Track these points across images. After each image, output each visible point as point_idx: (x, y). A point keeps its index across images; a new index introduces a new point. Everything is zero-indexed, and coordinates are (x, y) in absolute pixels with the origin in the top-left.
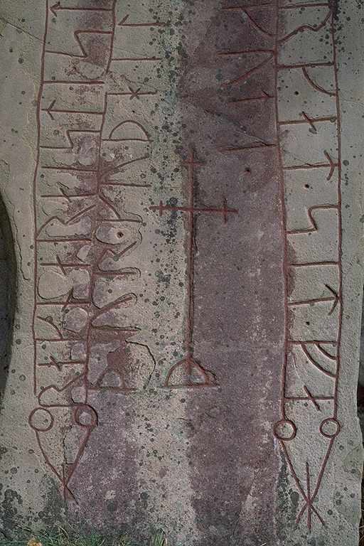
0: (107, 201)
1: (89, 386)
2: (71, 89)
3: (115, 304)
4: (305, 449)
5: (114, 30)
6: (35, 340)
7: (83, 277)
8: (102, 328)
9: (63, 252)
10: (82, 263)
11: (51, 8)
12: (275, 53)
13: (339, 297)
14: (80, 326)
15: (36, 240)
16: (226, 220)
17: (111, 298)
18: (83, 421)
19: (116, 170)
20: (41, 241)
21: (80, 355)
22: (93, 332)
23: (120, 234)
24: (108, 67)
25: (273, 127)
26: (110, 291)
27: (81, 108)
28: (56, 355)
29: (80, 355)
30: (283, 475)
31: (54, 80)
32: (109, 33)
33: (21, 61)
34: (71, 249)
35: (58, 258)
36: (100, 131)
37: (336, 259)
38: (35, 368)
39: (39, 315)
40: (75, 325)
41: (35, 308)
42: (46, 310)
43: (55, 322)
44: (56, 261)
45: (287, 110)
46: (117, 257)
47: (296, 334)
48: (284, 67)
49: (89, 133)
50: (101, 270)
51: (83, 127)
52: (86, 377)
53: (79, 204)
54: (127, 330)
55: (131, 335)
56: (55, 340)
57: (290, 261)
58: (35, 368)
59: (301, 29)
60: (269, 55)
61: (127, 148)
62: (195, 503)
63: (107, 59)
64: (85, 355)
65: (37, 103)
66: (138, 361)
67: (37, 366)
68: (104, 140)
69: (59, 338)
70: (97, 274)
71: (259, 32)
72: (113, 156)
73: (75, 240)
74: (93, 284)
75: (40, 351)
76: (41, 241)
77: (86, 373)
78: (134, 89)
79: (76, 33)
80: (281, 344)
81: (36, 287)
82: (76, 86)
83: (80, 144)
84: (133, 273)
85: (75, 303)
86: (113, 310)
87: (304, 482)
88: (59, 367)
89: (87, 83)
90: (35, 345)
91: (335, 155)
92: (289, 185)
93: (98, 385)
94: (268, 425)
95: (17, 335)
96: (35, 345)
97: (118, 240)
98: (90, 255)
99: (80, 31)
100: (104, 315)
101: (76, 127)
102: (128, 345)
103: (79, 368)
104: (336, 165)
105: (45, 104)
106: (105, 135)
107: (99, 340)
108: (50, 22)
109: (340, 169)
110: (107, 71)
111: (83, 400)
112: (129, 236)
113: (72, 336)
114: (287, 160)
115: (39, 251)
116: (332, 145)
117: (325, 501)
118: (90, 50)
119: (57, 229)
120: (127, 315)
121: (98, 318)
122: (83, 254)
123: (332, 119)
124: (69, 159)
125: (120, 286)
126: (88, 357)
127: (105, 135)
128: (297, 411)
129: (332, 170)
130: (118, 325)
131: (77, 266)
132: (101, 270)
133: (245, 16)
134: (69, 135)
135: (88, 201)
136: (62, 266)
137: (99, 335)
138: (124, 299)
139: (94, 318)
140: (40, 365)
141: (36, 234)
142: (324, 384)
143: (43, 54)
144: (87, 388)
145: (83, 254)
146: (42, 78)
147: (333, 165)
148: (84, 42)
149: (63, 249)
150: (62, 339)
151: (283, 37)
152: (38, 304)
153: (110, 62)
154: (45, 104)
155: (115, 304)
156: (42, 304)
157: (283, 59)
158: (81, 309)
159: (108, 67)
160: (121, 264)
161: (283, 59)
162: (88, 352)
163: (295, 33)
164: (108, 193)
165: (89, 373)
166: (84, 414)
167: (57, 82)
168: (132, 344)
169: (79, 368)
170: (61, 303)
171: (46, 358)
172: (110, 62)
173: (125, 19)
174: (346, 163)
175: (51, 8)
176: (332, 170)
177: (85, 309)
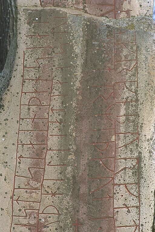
2: (26, 192)
5: (45, 167)
11: (19, 157)
12: (113, 179)
19: (45, 227)
24: (42, 183)
25: (111, 210)
27: (30, 200)
31: (19, 188)
32: (43, 168)
33: (5, 180)
36: (39, 210)
45: (118, 203)
48: (117, 184)
49: (33, 210)
51: (31, 208)
59: (125, 169)
60: (111, 179)
61: (50, 217)
63: (42, 179)
65: (12, 198)
68: (40, 214)
71: (107, 169)
72: (43, 220)
78: (53, 192)
79: (29, 168)
82: (28, 191)
89: (33, 189)
91: (137, 222)
99: (31, 168)
101: (28, 208)
104: (138, 226)
105: (15, 198)
106: (41, 212)
108: (18, 163)
109: (139, 227)
110: (42, 184)
114: (117, 224)
116: (136, 217)
118: (35, 176)
123: (137, 207)
124: (25, 222)
127: (41, 212)
129: (136, 228)
133: (101, 162)
134: (25, 211)
143: (15, 177)
146: (14, 187)
147: (136, 226)
148: (32, 172)
151: (117, 172)
153: (43, 181)
154: (15, 198)
157: (116, 181)
159: (42, 183)
161: (116, 181)
163: (122, 170)
167: (21, 189)
172: (43, 181)
173: (49, 163)
174: (142, 225)
175: (19, 157)
176: (136, 228)
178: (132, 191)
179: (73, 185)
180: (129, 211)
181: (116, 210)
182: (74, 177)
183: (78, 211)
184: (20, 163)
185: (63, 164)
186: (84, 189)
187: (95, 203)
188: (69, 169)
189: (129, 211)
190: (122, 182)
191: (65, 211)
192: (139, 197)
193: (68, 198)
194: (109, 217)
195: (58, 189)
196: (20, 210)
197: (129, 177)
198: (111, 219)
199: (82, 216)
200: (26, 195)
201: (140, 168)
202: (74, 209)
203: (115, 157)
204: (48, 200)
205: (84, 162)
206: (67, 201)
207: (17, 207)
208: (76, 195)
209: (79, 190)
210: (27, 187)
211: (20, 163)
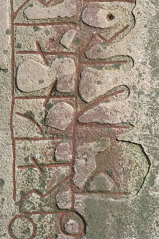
1: (76, 190)
3: (104, 98)
6: (14, 140)
7: (69, 67)
8: (91, 124)
9: (45, 40)
10: (65, 50)
14: (65, 122)
15: (13, 24)
17: (100, 90)
18: (69, 229)
20: (18, 24)
21: (65, 156)
22: (80, 129)
23: (111, 17)
26: (99, 83)
28: (37, 156)
29: (65, 156)
34: (54, 34)
35: (38, 45)
38: (14, 170)
39: (18, 110)
40: (60, 122)
41: (13, 103)
43: (36, 118)
44: (35, 48)
46: (107, 42)
52: (71, 181)
54: (118, 127)
55: (122, 132)
56: (36, 139)
58: (14, 170)
64: (71, 156)
66: (130, 162)
67: (16, 168)
69: (40, 136)
70: (85, 63)
73: (59, 23)
74: (80, 75)
75: (19, 152)
76: (18, 24)
77: (72, 176)
81: (15, 80)
84: (125, 62)
85: (59, 97)
86: (101, 105)
88: (41, 170)
90: (14, 144)
93: (87, 190)
96: (14, 144)
97: (107, 23)
98: (76, 41)
100: (91, 111)
102: (119, 144)
103: (64, 170)
107: (87, 139)
111: (69, 206)
112: (121, 18)
113: (56, 135)
115: (18, 37)
120: (119, 109)
121: (85, 113)
122: (68, 41)
125: (110, 78)
126: (74, 157)
130: (108, 122)
131: (61, 55)
132: (85, 57)
136: (43, 54)
137: (86, 131)
138: (114, 92)
139: (82, 113)
140: (19, 167)
141: (13, 16)
144: (74, 192)
145: (68, 41)
149: (44, 35)
150: (44, 138)
152: (17, 98)
155: (104, 98)
156: (21, 98)
158: (65, 103)
160: (110, 52)
162: (75, 152)
165: (77, 174)
166: (71, 221)
168: (124, 143)
169: (64, 170)
170: (42, 97)
171: (26, 159)
177: (71, 104)
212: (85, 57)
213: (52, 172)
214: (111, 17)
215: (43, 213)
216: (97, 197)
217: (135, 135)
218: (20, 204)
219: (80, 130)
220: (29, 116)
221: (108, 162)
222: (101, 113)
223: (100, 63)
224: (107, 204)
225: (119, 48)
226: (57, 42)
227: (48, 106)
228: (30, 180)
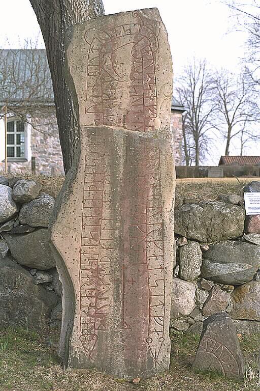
0: (100, 279)
3: (102, 307)
4: (155, 345)
7: (94, 300)
13: (164, 305)
16: (133, 284)
17: (101, 306)
23: (104, 288)
30: (149, 353)
33: (75, 240)
34: (90, 292)
37: (163, 294)
42: (84, 309)
46: (102, 294)
47: (152, 316)
50: (99, 297)
53: (92, 280)
57: (151, 295)
59: (153, 231)
62: (125, 360)
65: (80, 252)
80: (148, 318)
81: (81, 303)
83: (92, 263)
87: (154, 354)
92: (150, 274)
94: (144, 339)
95: (76, 316)
97: (103, 290)
103: (93, 324)
113: (91, 316)
114: (149, 267)
117: (160, 359)
119: (86, 287)
120: (106, 310)
122: (93, 294)
128: (152, 335)
132: (99, 297)
135: (94, 279)
138: (105, 306)
142: (159, 328)
145: (93, 294)
148: (93, 235)
155: (102, 307)
160: (103, 296)
161: (148, 239)
164: (100, 277)
174: (166, 268)
178: (158, 246)
179: (119, 243)
180: (157, 259)
181: (149, 258)
182: (120, 237)
183: (123, 260)
184: (84, 229)
185: (113, 229)
186: (127, 245)
187: (134, 254)
188: (117, 232)
189: (157, 259)
190: (152, 240)
191: (115, 260)
192: (163, 249)
193: (117, 251)
194: (144, 263)
195: (110, 245)
196: (85, 260)
197: (156, 236)
198: (146, 264)
199: (126, 263)
200: (89, 250)
201: (163, 230)
202: (121, 258)
203: (146, 223)
204: (104, 252)
205: (126, 227)
206: (116, 254)
207: (83, 258)
208: (122, 249)
209: (123, 246)
210: (90, 245)
211: (84, 229)
212: (97, 298)
213: (89, 325)
214: (104, 288)
215: (88, 335)
216: (101, 331)
217: (110, 316)
218: (82, 333)
219: (97, 315)
220: (84, 311)
221: (103, 322)
222: (102, 311)
223: (101, 299)
224: (103, 333)
225: (103, 296)
226: (90, 294)
227: (89, 309)
228: (85, 327)
